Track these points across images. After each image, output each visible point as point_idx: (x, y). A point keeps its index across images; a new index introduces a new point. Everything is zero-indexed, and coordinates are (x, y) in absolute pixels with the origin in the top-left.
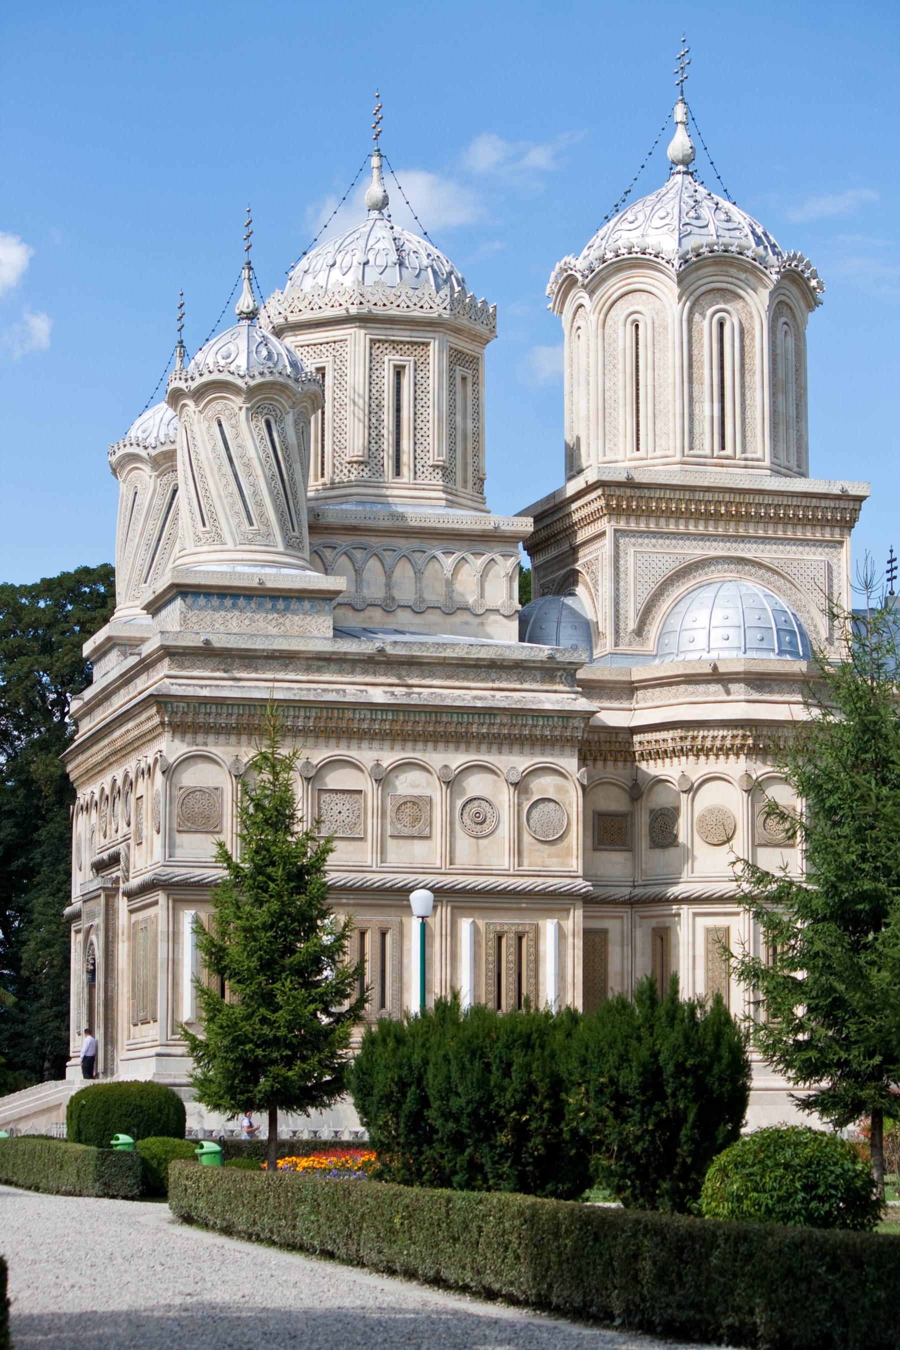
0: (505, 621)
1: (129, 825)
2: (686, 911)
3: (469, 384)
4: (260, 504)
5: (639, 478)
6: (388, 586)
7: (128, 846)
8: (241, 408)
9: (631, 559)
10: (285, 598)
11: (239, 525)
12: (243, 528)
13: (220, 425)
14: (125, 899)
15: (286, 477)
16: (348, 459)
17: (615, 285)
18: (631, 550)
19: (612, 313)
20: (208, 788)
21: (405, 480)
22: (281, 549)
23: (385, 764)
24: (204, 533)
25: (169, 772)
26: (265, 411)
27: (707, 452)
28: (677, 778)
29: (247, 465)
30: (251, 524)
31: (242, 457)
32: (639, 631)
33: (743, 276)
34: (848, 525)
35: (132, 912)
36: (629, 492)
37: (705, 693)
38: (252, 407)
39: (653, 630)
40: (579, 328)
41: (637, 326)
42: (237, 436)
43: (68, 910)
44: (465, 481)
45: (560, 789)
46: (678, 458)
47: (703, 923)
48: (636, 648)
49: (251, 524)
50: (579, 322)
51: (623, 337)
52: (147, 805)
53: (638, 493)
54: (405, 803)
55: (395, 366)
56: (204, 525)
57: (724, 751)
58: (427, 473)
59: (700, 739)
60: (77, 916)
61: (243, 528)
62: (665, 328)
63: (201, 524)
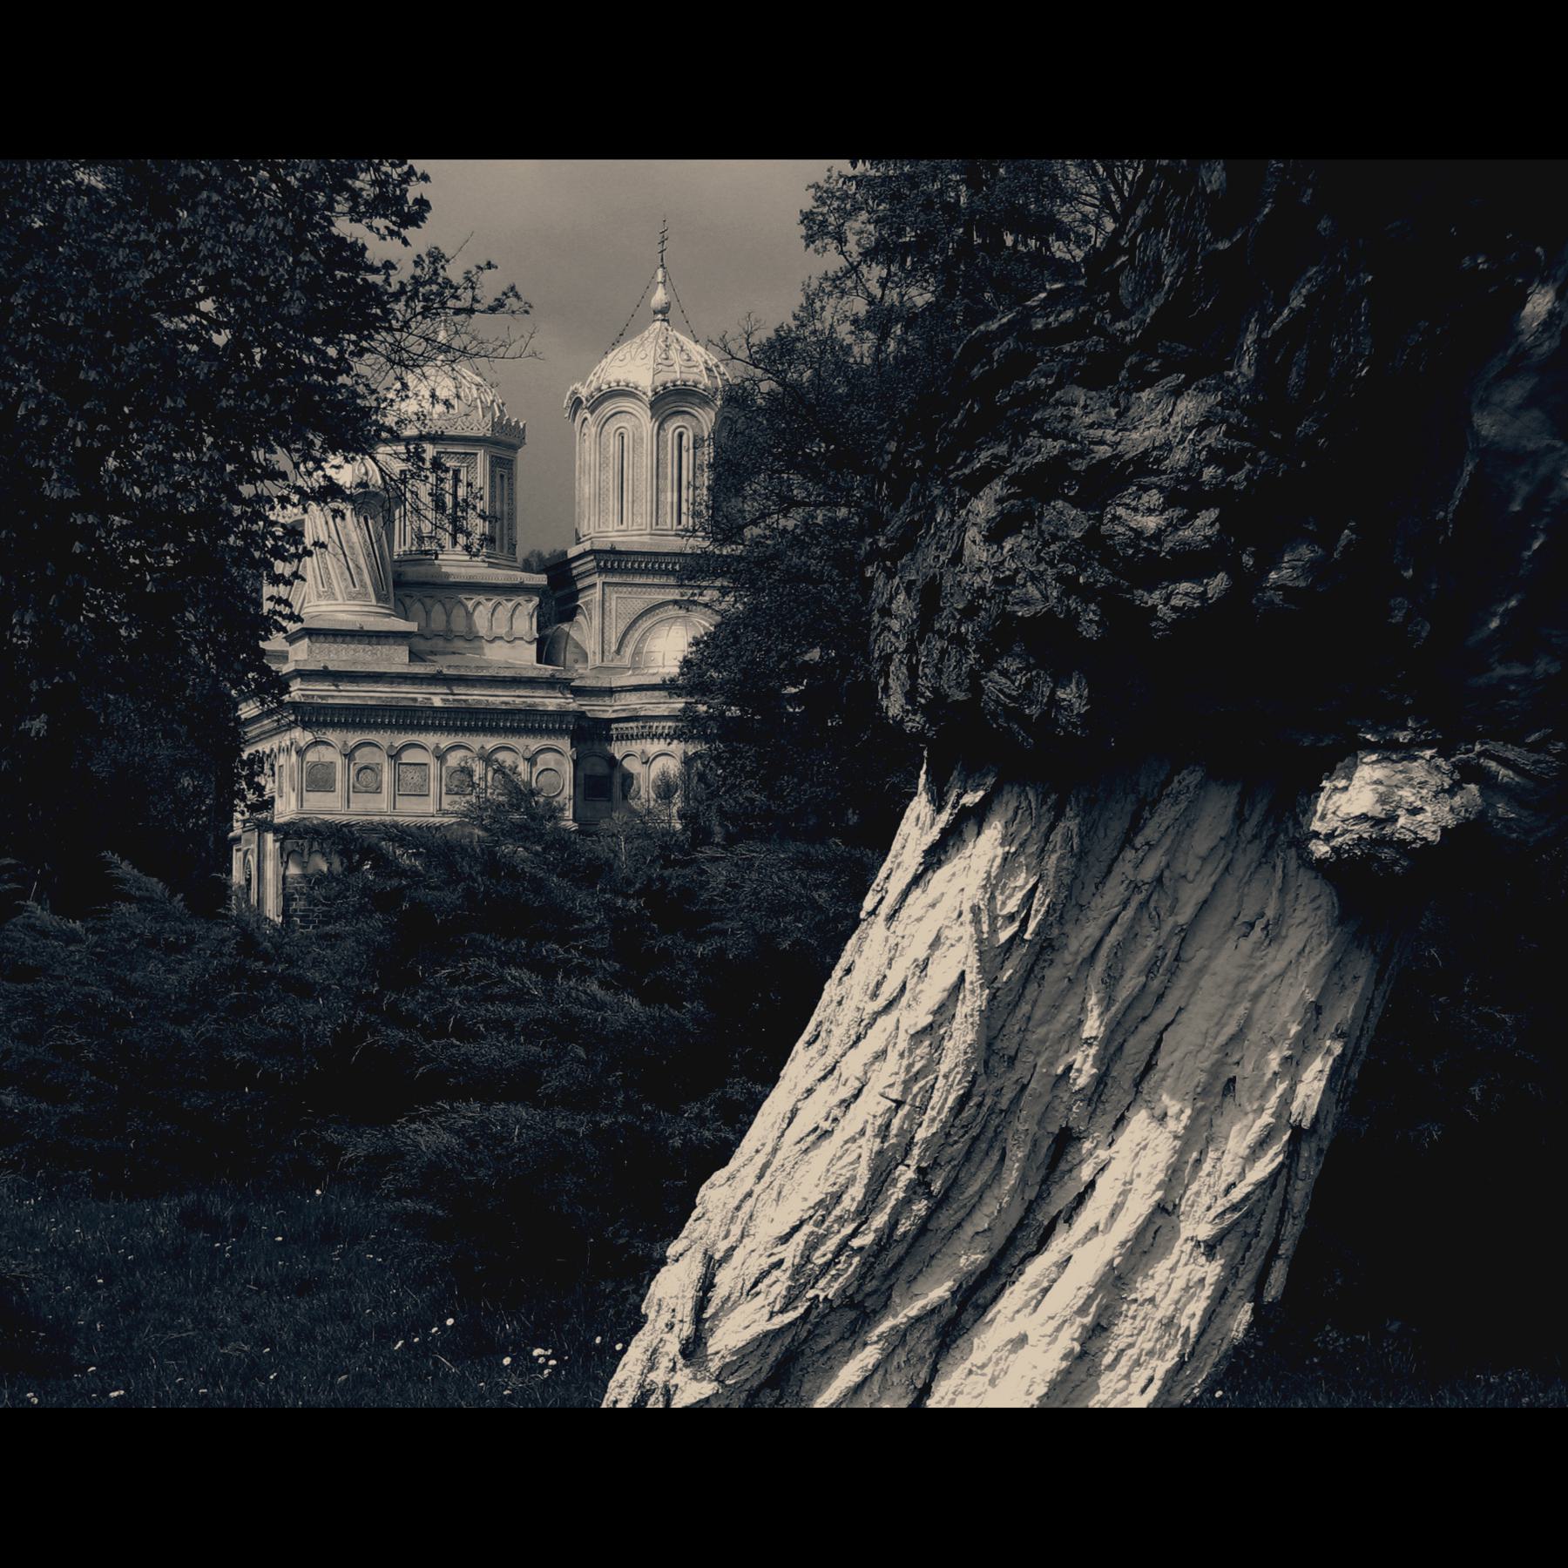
0: (527, 646)
3: (506, 480)
6: (448, 622)
9: (614, 603)
11: (346, 587)
17: (608, 408)
18: (613, 597)
19: (606, 427)
22: (374, 602)
23: (442, 746)
25: (301, 753)
29: (351, 548)
32: (618, 652)
39: (628, 651)
42: (345, 527)
43: (231, 834)
45: (558, 763)
46: (648, 531)
48: (616, 663)
50: (585, 430)
51: (613, 445)
52: (286, 772)
53: (618, 557)
60: (237, 840)
62: (642, 439)
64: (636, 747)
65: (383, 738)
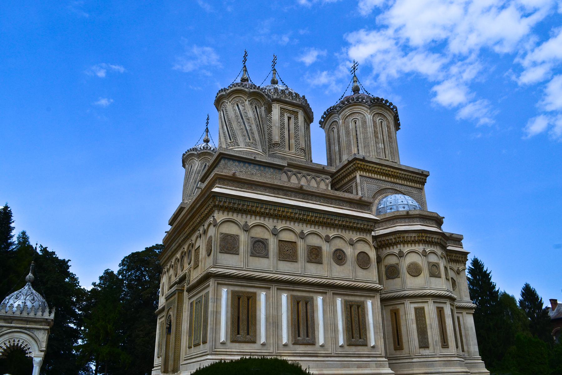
1: (189, 264)
2: (407, 302)
4: (253, 133)
5: (367, 159)
7: (190, 271)
8: (246, 100)
10: (263, 166)
11: (245, 139)
12: (246, 141)
13: (238, 106)
14: (187, 293)
15: (262, 127)
16: (273, 143)
19: (347, 120)
20: (233, 235)
21: (293, 152)
24: (230, 142)
26: (255, 103)
27: (382, 158)
28: (397, 253)
30: (250, 140)
31: (246, 116)
33: (386, 111)
34: (423, 183)
35: (189, 299)
36: (364, 163)
37: (405, 222)
38: (250, 100)
40: (333, 128)
41: (355, 123)
44: (308, 159)
47: (413, 306)
49: (250, 140)
54: (313, 249)
55: (288, 117)
56: (231, 140)
57: (414, 242)
58: (299, 151)
59: (406, 238)
61: (246, 141)
63: (229, 140)
64: (396, 250)
65: (269, 223)
